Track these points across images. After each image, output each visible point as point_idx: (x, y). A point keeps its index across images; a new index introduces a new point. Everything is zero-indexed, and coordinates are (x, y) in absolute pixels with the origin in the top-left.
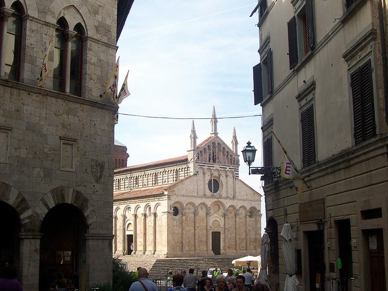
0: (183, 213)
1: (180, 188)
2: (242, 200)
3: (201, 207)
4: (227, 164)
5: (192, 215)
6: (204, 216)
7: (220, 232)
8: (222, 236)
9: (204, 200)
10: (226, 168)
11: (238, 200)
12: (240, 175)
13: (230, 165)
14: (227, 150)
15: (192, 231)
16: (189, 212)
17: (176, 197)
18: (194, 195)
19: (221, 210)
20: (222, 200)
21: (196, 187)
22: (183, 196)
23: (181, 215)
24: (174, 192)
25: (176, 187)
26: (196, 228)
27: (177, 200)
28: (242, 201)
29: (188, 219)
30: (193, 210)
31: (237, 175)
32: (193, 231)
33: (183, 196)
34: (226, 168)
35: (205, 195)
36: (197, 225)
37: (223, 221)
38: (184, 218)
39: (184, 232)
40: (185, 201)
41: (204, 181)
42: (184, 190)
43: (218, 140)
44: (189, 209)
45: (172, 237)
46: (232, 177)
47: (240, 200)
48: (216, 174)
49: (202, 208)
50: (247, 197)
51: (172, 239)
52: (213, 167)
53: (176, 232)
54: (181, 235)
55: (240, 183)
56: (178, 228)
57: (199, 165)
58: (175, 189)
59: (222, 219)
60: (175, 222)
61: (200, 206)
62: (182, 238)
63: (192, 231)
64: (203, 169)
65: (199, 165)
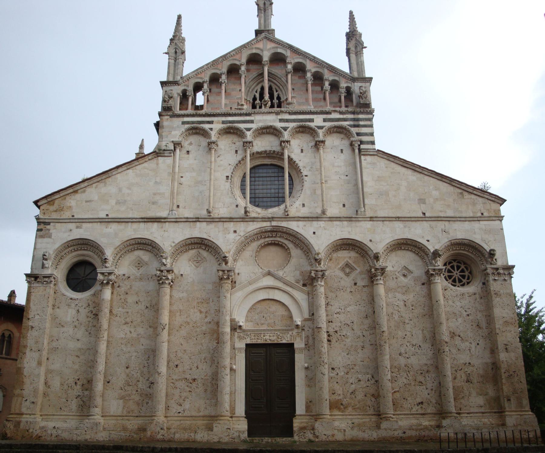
1: (96, 198)
2: (398, 219)
3: (199, 255)
4: (312, 108)
7: (290, 346)
8: (300, 361)
10: (312, 120)
11: (372, 219)
12: (377, 138)
13: (329, 108)
14: (311, 67)
17: (72, 226)
19: (293, 261)
20: (293, 226)
21: (165, 189)
22: (107, 221)
28: (398, 225)
31: (365, 139)
33: (107, 221)
34: (312, 120)
37: (304, 304)
40: (109, 238)
42: (113, 202)
43: (270, 45)
46: (347, 151)
47: (384, 219)
48: (263, 144)
50: (423, 208)
52: (252, 122)
53: (72, 345)
55: (382, 163)
57: (184, 123)
59: (301, 297)
60: (72, 312)
61: (192, 252)
63: (143, 341)
64: (205, 134)
65: (184, 123)
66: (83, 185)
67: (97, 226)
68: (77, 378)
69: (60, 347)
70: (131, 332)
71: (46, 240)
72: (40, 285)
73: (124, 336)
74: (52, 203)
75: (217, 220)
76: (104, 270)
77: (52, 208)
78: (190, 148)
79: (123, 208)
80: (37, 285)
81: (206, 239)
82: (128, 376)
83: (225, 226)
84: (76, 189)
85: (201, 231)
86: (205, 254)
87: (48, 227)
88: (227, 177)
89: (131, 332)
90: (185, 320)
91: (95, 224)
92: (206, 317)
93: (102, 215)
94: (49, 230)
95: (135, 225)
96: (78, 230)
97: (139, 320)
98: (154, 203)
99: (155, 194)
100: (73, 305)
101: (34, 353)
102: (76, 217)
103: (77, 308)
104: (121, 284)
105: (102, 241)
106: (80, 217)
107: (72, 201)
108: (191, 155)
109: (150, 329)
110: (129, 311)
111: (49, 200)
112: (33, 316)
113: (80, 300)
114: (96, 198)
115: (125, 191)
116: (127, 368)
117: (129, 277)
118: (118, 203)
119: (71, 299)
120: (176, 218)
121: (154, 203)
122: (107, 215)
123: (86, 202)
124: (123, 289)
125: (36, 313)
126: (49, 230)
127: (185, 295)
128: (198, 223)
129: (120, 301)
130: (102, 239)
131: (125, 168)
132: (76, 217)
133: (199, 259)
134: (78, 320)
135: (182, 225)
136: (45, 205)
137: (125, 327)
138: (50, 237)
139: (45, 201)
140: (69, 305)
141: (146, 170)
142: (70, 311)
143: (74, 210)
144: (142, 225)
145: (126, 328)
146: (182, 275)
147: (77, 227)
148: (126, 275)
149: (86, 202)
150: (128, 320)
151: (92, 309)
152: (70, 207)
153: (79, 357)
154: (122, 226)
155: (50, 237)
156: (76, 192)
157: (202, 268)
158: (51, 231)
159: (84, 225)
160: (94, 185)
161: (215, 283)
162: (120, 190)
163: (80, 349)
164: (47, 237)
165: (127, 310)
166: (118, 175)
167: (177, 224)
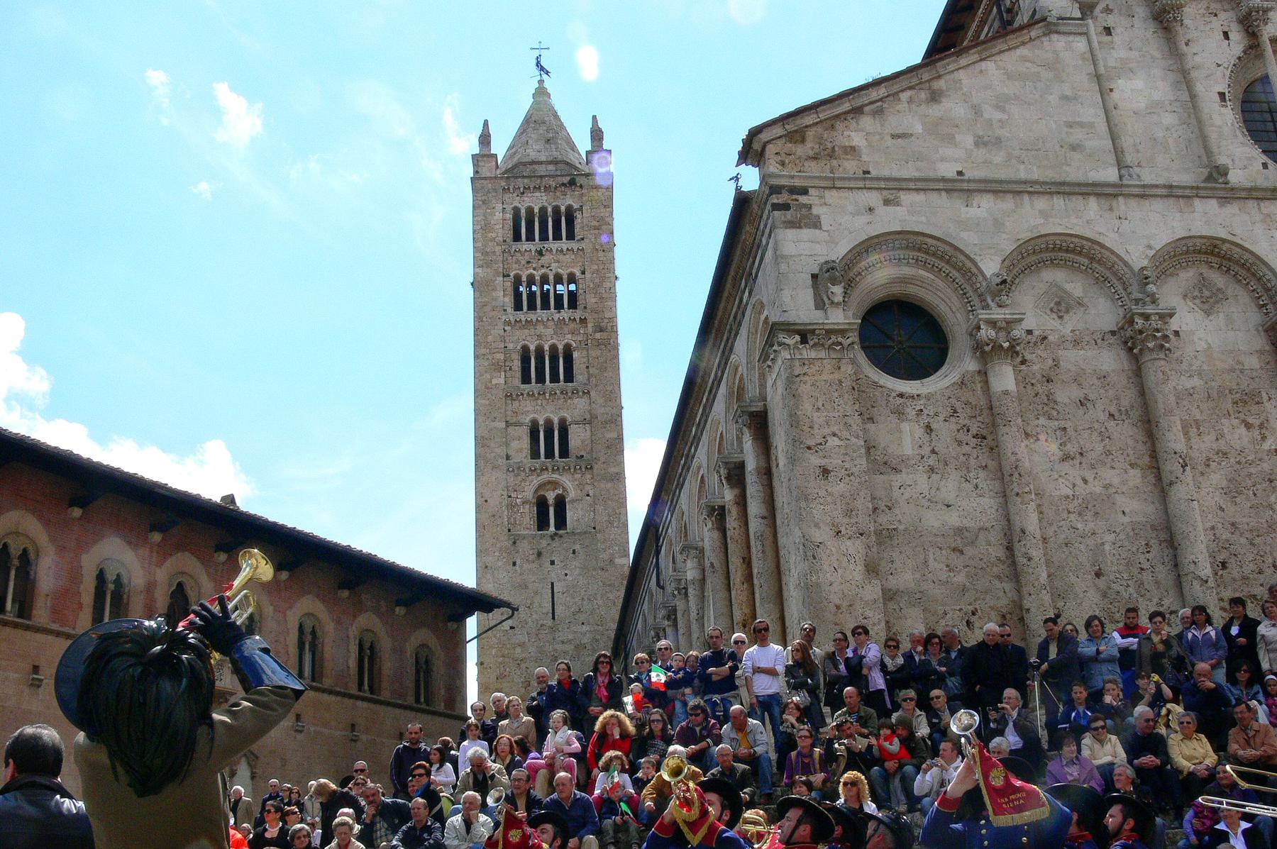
0: (986, 333)
1: (918, 128)
3: (1203, 282)
5: (1110, 360)
6: (1253, 362)
9: (1208, 218)
15: (1122, 502)
16: (1068, 328)
17: (873, 198)
18: (1074, 173)
21: (1090, 112)
22: (959, 187)
23: (971, 365)
24: (850, 166)
25: (867, 122)
26: (1171, 467)
27: (891, 219)
29: (1065, 395)
30: (1102, 313)
32: (1134, 506)
33: (959, 187)
35: (1215, 182)
36: (1174, 439)
38: (1005, 378)
39: (1030, 520)
41: (1184, 77)
42: (969, 141)
44: (1061, 305)
45: (872, 569)
49: (1208, 300)
51: (872, 591)
54: (997, 552)
56: (950, 487)
58: (857, 139)
61: (1187, 276)
62: (1016, 575)
66: (874, 94)
67: (941, 200)
68: (971, 608)
69: (901, 527)
70: (1085, 481)
71: (806, 233)
72: (822, 354)
73: (1070, 492)
74: (797, 137)
75: (1243, 194)
76: (998, 314)
77: (800, 150)
78: (1110, 21)
79: (999, 158)
80: (813, 354)
81: (1224, 241)
82: (1104, 595)
83: (1265, 211)
84: (858, 102)
85: (1208, 218)
86: (1218, 279)
87: (803, 199)
88: (1222, 95)
89: (1085, 481)
90: (1215, 446)
91: (934, 196)
92: (1264, 438)
93: (948, 170)
94: (809, 207)
95: (1041, 203)
96: (890, 209)
97: (1099, 448)
98: (1074, 148)
99: (1070, 125)
100: (911, 413)
101: (849, 543)
102: (874, 173)
103: (924, 420)
104: (1028, 357)
105: (967, 240)
106: (885, 173)
107: (855, 135)
108: (1117, 38)
109: (1132, 472)
110: (1068, 425)
111: (790, 127)
112: (822, 440)
113: (928, 397)
114: (918, 128)
115: (990, 113)
116: (1098, 574)
117: (1045, 338)
118: (980, 142)
119: (901, 395)
120: (1144, 186)
121: (1074, 148)
122: (960, 173)
123: (894, 136)
124: (1036, 368)
125: (827, 431)
126: (809, 207)
127: (1197, 382)
128: (1197, 202)
129: (1037, 400)
130: (964, 235)
131: (976, 57)
132: (874, 173)
133: (1207, 293)
134: (933, 452)
135: (1158, 205)
136: (780, 142)
137: (1066, 467)
138: (816, 224)
139: (778, 131)
140: (899, 413)
141: (1029, 65)
142: (906, 426)
143: (865, 158)
144: (1058, 202)
145: (1072, 471)
146: (1177, 333)
147: (887, 202)
148: (1036, 333)
149: (894, 136)
150: (1072, 448)
151: (967, 422)
152: (853, 148)
153: (962, 552)
154: (1007, 204)
155: (816, 224)
156: (858, 111)
157: (1221, 315)
158: (815, 211)
159: (906, 198)
160: (904, 96)
161: (1261, 352)
162: (977, 111)
163: (959, 531)
164: (807, 226)
165: (1063, 424)
166: (961, 74)
167: (1142, 202)
